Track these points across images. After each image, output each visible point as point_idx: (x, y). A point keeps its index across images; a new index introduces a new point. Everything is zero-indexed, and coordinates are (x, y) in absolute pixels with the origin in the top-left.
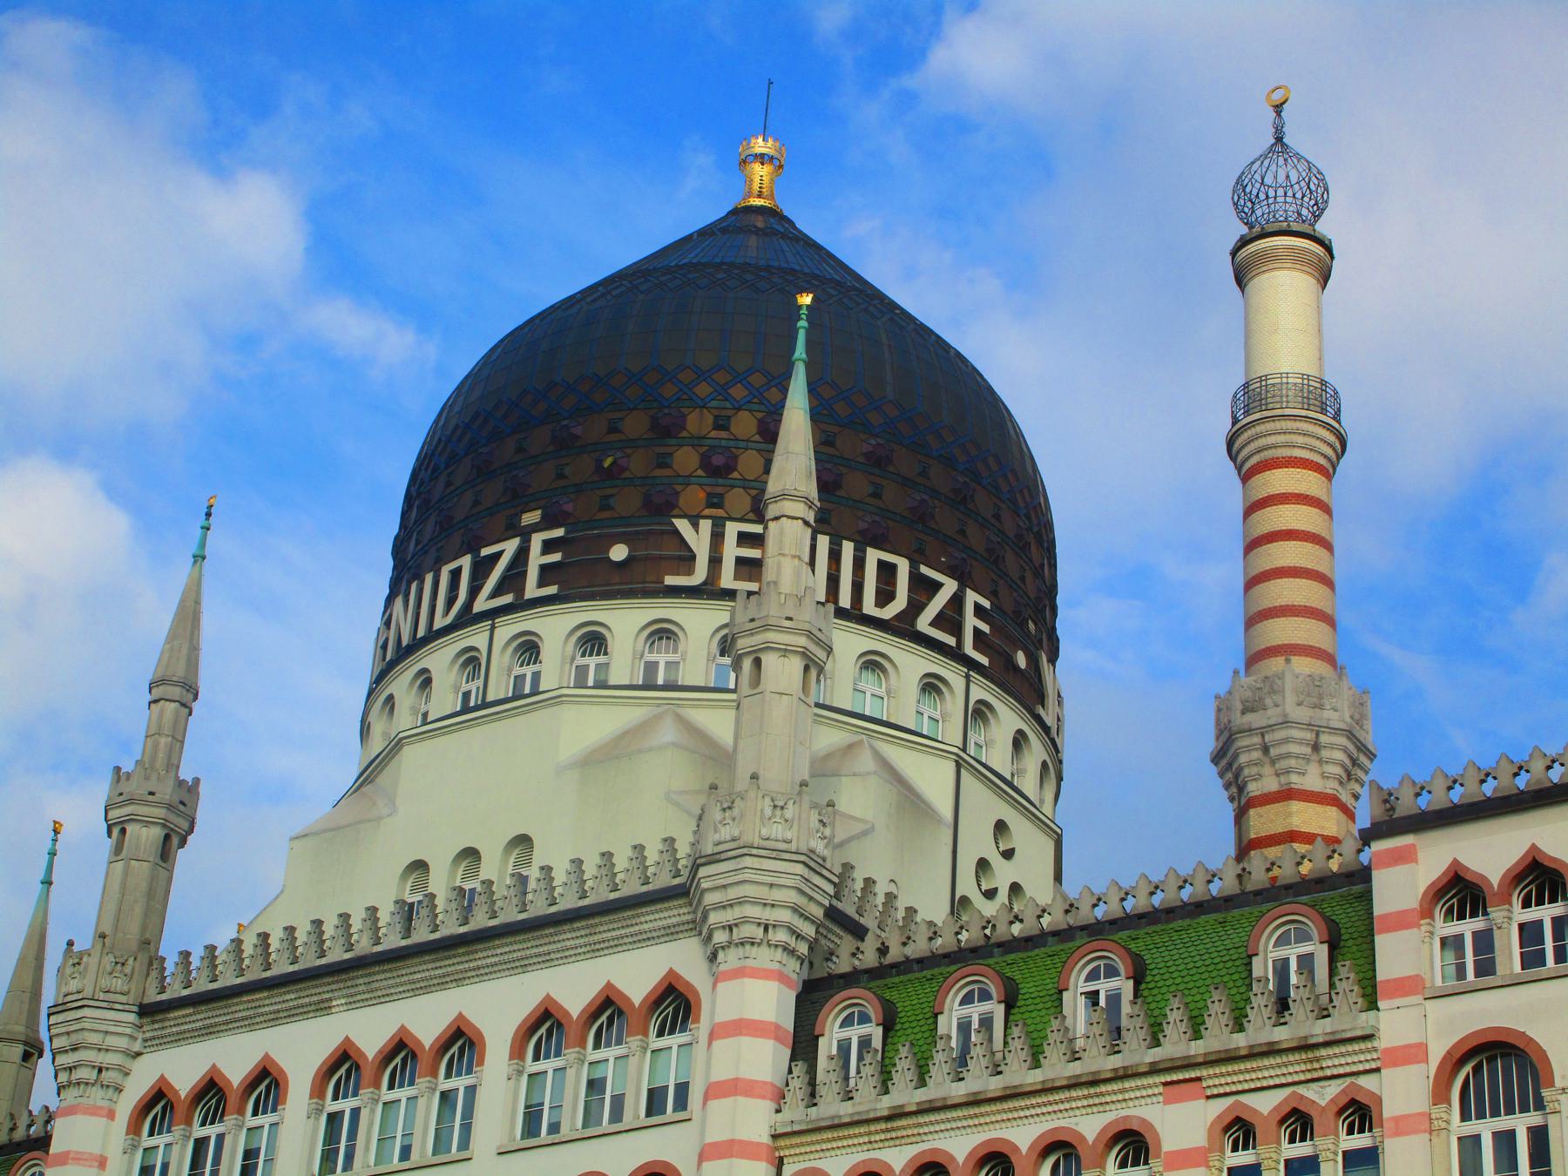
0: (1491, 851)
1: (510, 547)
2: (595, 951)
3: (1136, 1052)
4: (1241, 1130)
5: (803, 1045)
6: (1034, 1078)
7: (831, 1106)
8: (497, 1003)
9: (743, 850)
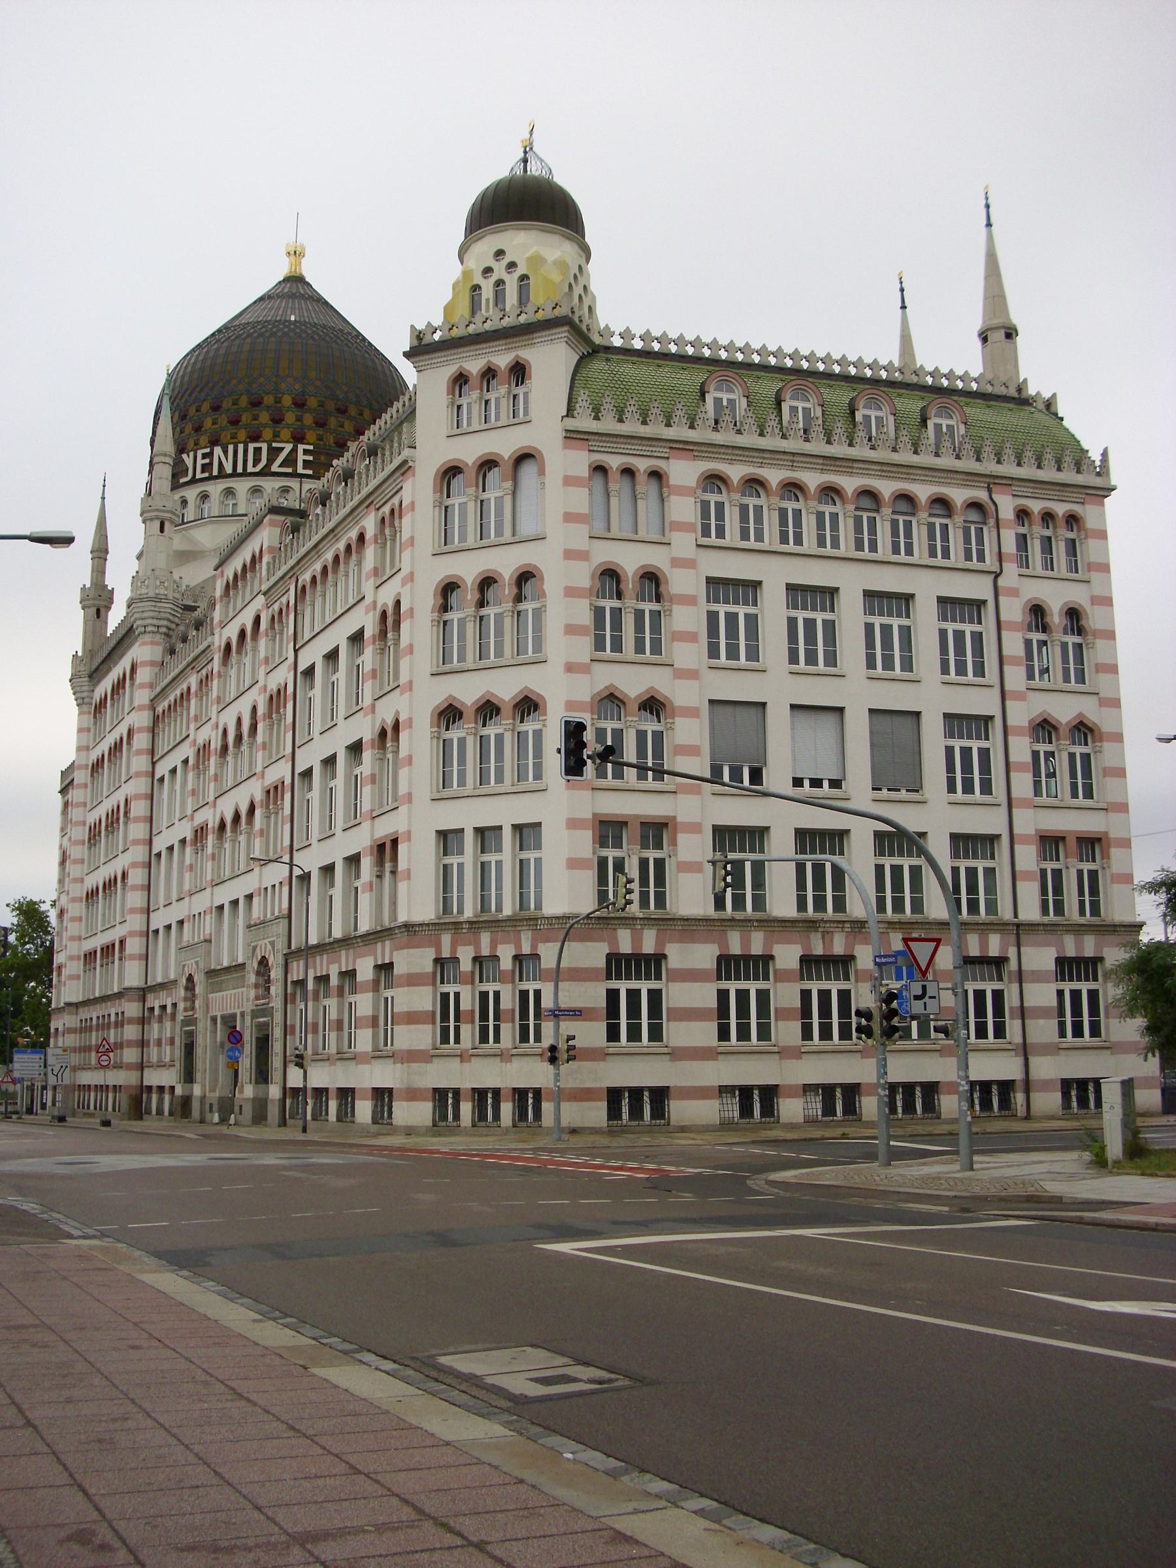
1: (288, 447)
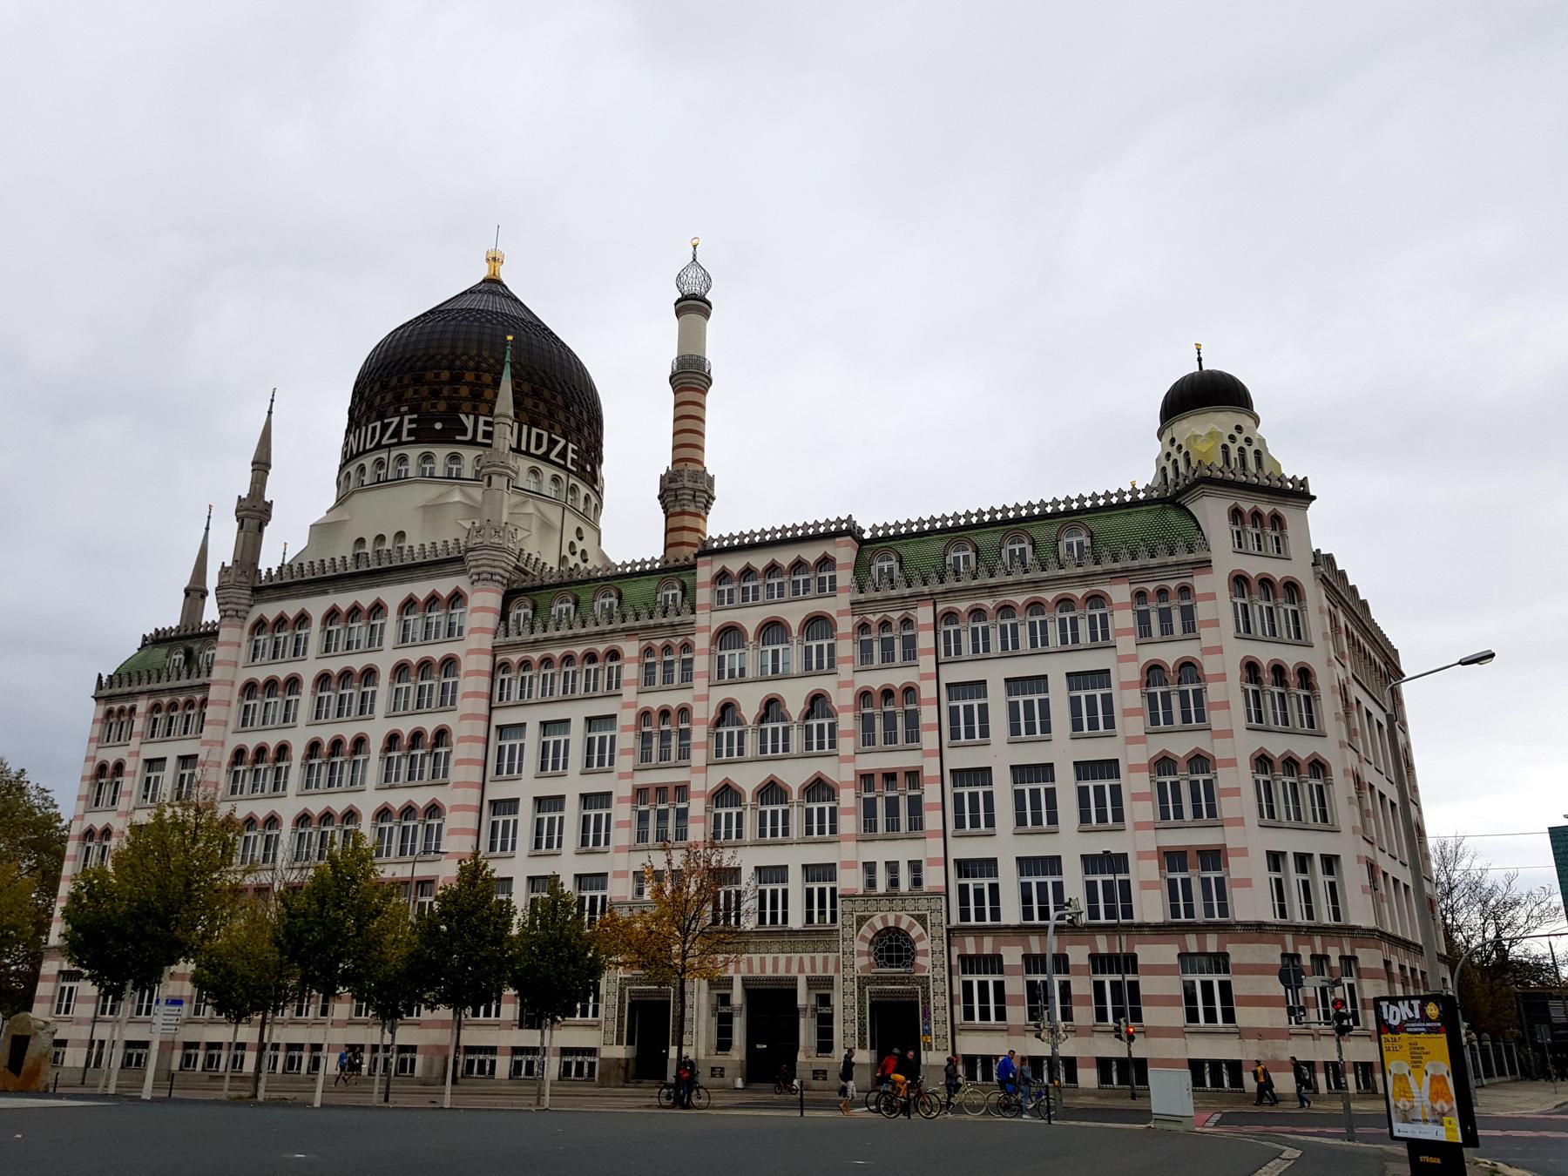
0: (735, 564)
1: (396, 420)
2: (429, 578)
3: (618, 624)
4: (648, 651)
5: (504, 616)
6: (583, 631)
7: (513, 638)
8: (393, 595)
9: (486, 547)
